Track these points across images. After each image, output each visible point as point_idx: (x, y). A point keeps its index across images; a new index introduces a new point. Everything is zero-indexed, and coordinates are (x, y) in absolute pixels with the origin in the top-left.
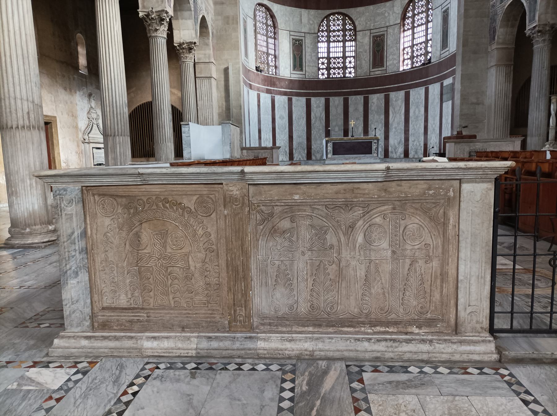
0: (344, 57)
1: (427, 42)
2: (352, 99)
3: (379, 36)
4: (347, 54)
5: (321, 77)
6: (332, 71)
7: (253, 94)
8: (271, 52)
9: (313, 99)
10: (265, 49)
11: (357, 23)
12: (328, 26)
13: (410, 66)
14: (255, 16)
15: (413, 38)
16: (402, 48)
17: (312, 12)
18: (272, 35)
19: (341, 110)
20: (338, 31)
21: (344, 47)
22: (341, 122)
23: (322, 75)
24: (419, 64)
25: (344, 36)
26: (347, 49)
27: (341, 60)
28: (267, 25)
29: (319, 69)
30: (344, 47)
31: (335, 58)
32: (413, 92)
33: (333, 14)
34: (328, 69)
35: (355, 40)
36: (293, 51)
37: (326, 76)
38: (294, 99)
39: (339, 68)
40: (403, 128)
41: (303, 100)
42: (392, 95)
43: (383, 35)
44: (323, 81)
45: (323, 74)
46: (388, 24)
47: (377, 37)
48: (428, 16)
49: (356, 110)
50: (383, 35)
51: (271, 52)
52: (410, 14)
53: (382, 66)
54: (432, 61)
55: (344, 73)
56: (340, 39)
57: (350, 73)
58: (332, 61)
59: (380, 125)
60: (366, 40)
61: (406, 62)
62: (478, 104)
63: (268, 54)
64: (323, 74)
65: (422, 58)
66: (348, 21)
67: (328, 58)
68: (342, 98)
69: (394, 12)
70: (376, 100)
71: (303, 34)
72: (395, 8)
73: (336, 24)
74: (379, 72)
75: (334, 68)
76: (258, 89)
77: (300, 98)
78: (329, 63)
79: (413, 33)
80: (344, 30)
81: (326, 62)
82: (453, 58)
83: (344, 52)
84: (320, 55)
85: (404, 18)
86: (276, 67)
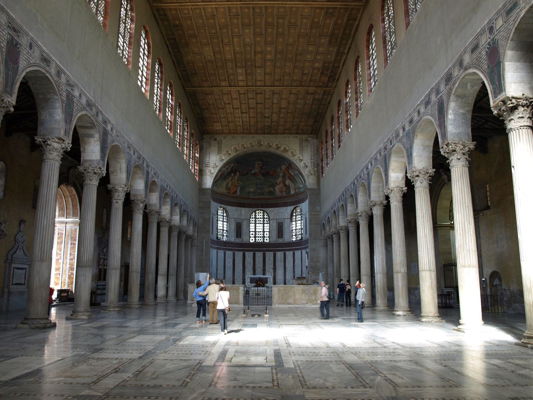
0: (264, 232)
1: (301, 229)
2: (267, 253)
3: (281, 223)
4: (265, 230)
5: (251, 241)
6: (257, 238)
7: (215, 251)
8: (225, 229)
9: (247, 253)
10: (222, 228)
11: (270, 216)
12: (255, 215)
13: (295, 239)
14: (218, 212)
15: (296, 226)
16: (291, 229)
17: (247, 209)
18: (226, 220)
19: (261, 259)
20: (261, 218)
21: (264, 226)
22: (261, 265)
23: (252, 240)
24: (299, 239)
25: (264, 221)
26: (265, 228)
27: (262, 233)
28: (223, 216)
29: (250, 237)
30: (264, 226)
31: (258, 232)
32: (296, 252)
33: (258, 210)
34: (255, 237)
35: (269, 223)
36: (237, 229)
37: (254, 241)
38: (236, 253)
39: (261, 237)
40: (292, 270)
41: (241, 253)
42: (287, 253)
43: (283, 223)
44: (252, 244)
45: (252, 240)
46: (284, 218)
47: (280, 223)
48: (301, 217)
49: (270, 259)
50: (283, 223)
51: (225, 229)
52: (294, 214)
53: (282, 238)
54: (303, 238)
55: (264, 240)
56: (262, 222)
57: (267, 240)
58: (257, 233)
59: (282, 268)
60: (275, 224)
61: (294, 237)
62: (318, 262)
63: (223, 230)
64: (252, 240)
65: (300, 236)
66: (265, 214)
67: (255, 232)
68: (262, 253)
69: (287, 213)
70: (280, 255)
71: (242, 220)
72: (288, 211)
73: (260, 214)
74: (281, 241)
75: (258, 237)
76: (217, 248)
77: (239, 252)
78: (255, 234)
79: (296, 224)
80: (264, 218)
81: (254, 233)
82: (308, 239)
83: (264, 229)
84: (251, 230)
85: (292, 216)
86: (227, 236)
